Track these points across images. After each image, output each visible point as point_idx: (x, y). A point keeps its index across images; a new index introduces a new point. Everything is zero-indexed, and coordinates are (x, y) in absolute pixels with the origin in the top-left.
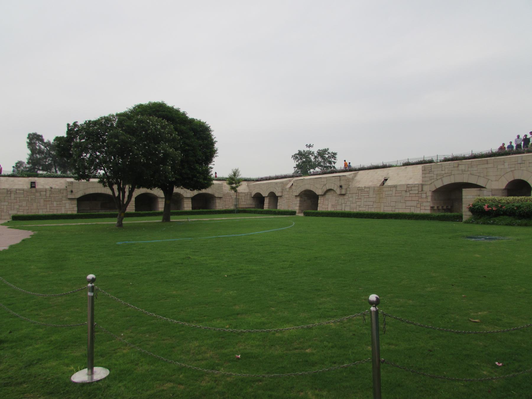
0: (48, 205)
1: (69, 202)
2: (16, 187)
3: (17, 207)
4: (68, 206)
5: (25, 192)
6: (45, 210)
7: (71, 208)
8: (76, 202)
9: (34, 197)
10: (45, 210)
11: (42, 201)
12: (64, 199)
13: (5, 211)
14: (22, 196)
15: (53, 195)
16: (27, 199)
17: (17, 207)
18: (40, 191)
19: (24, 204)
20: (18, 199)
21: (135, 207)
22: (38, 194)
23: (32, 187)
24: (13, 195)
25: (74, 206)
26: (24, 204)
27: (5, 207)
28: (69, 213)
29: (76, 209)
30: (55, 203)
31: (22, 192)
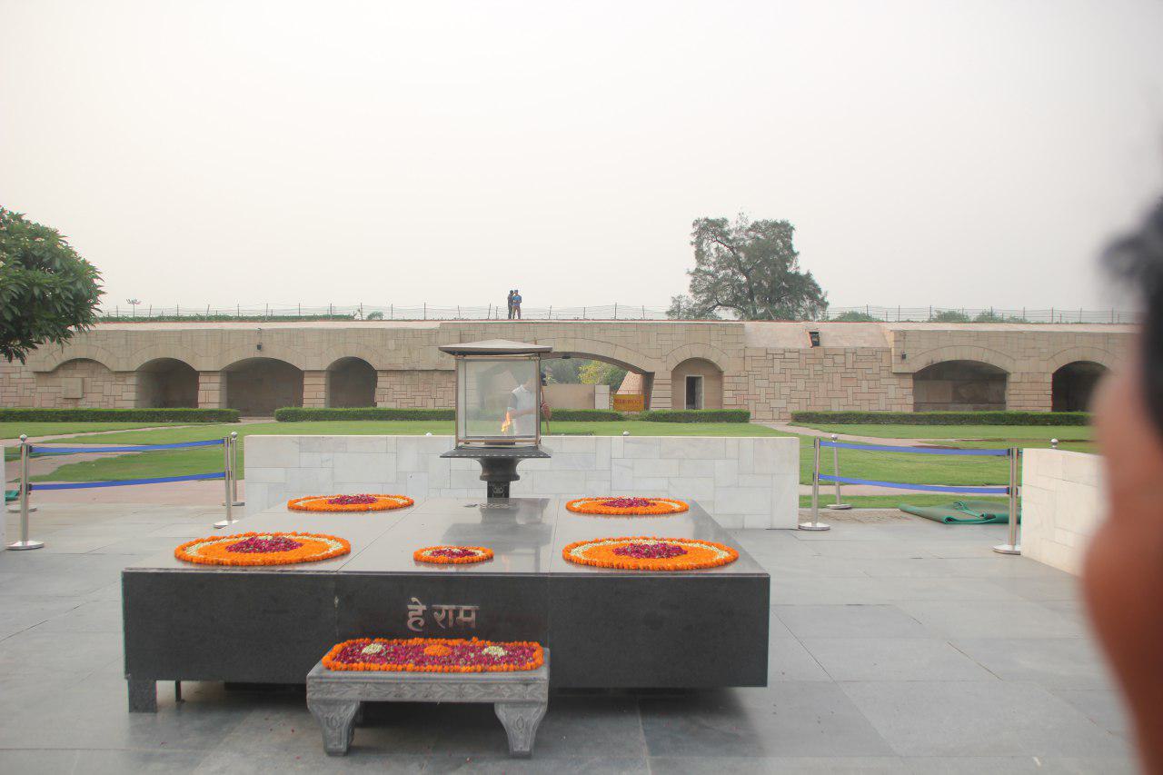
0: (850, 391)
1: (895, 381)
2: (782, 345)
3: (787, 391)
4: (892, 392)
5: (803, 357)
6: (843, 401)
7: (900, 398)
8: (909, 382)
9: (818, 367)
10: (843, 401)
11: (837, 378)
12: (884, 374)
13: (763, 400)
14: (797, 365)
15: (861, 365)
16: (806, 372)
17: (787, 391)
18: (831, 354)
19: (801, 385)
20: (788, 372)
21: (1053, 399)
22: (828, 362)
23: (816, 344)
24: (777, 362)
25: (905, 391)
26: (801, 385)
27: (763, 394)
28: (896, 410)
29: (911, 400)
30: (864, 383)
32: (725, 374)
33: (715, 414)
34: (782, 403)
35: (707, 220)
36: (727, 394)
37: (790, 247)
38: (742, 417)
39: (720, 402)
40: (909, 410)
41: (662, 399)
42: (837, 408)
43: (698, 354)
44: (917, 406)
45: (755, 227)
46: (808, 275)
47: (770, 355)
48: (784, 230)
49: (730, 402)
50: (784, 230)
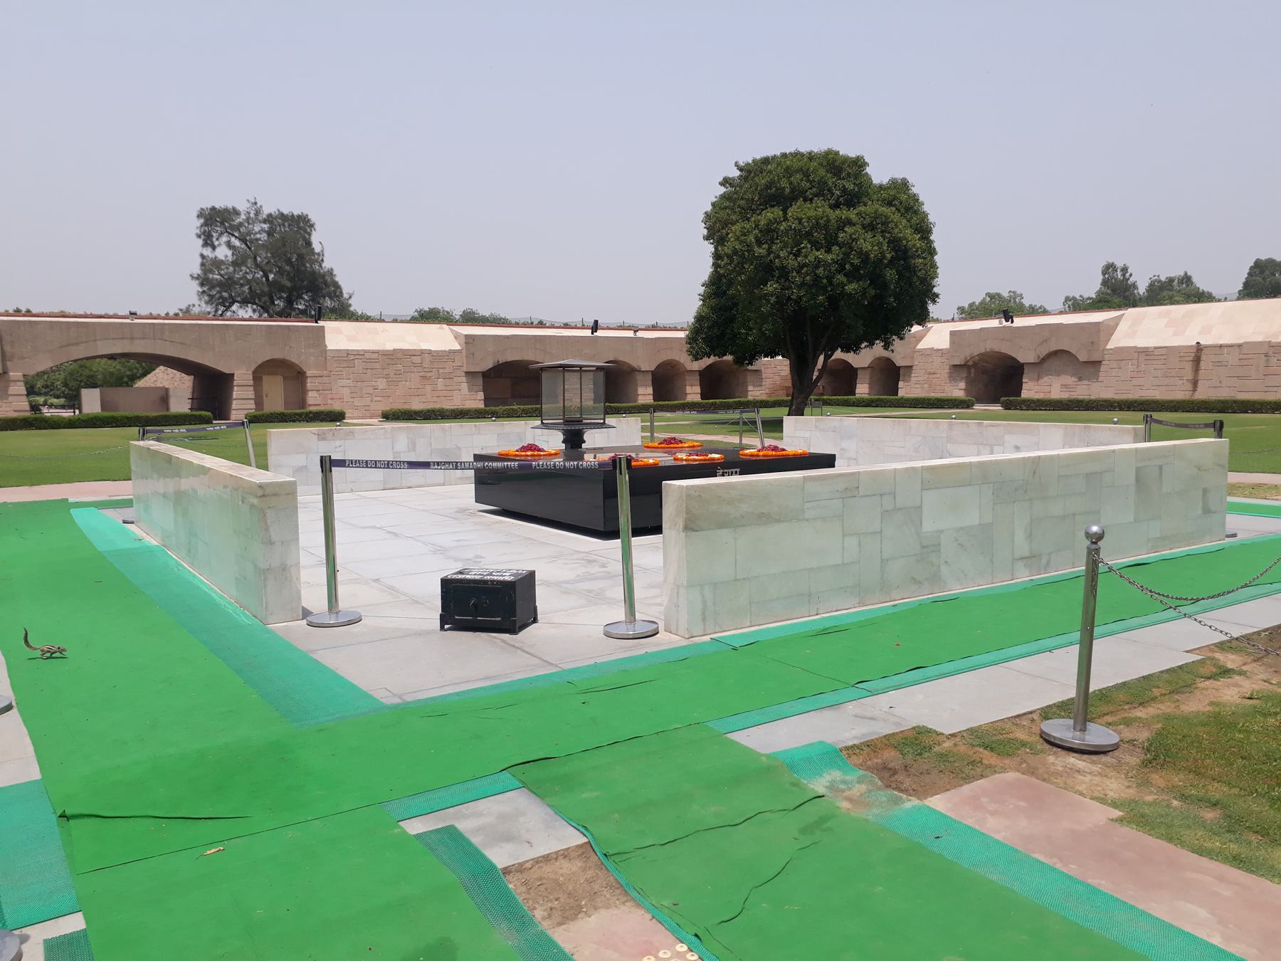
8: (480, 381)
14: (378, 366)
29: (481, 395)
31: (375, 356)
32: (309, 373)
33: (300, 415)
34: (367, 401)
35: (213, 209)
36: (310, 394)
37: (309, 244)
38: (336, 417)
39: (303, 403)
40: (481, 405)
41: (241, 402)
42: (417, 405)
43: (278, 355)
44: (487, 400)
45: (269, 219)
46: (330, 272)
47: (348, 357)
48: (299, 226)
49: (314, 401)
50: (299, 226)
